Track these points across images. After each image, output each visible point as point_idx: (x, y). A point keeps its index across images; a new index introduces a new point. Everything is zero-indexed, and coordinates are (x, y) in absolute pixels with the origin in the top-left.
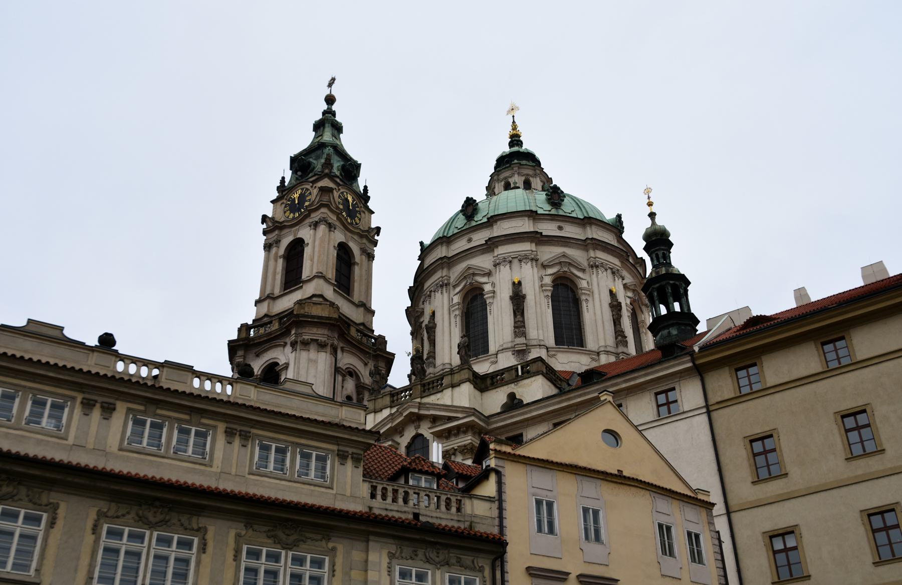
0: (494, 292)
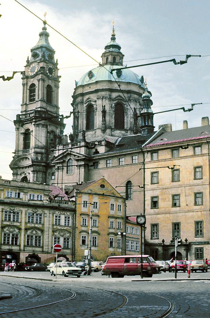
0: (97, 108)
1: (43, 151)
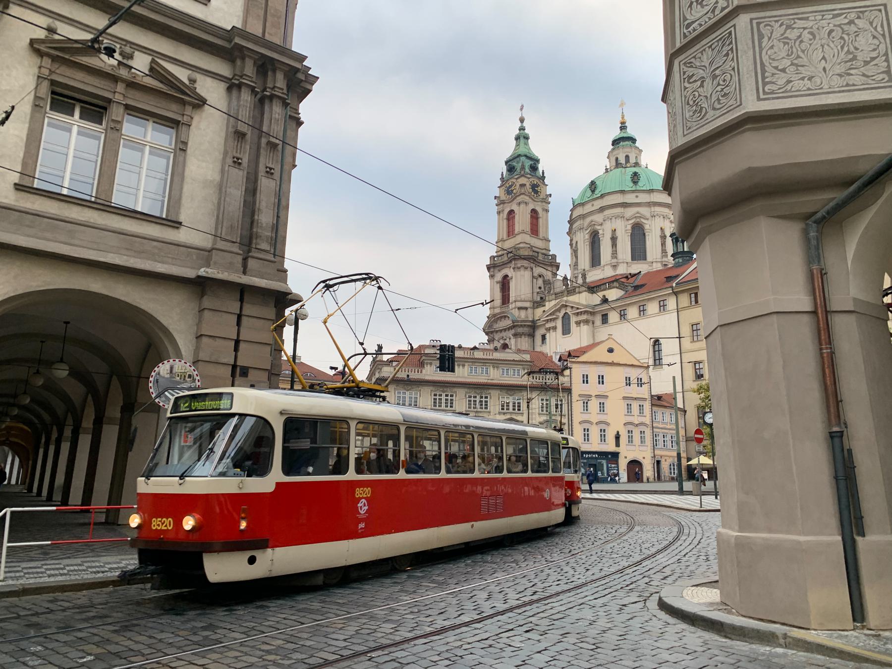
1: (527, 305)
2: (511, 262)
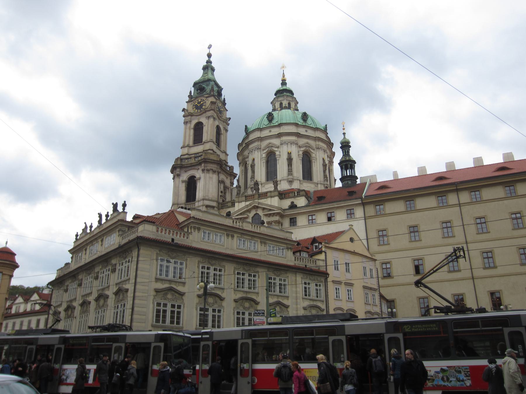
1: (214, 204)
2: (200, 164)
